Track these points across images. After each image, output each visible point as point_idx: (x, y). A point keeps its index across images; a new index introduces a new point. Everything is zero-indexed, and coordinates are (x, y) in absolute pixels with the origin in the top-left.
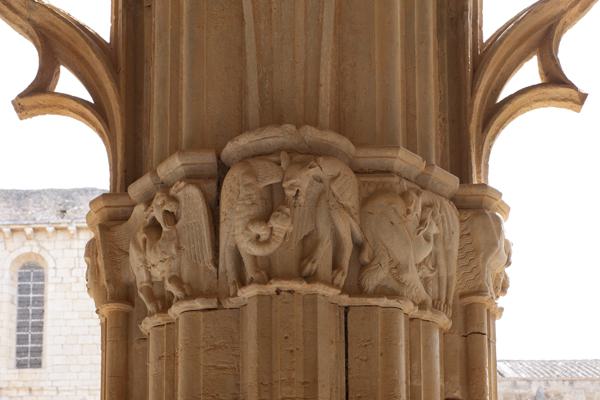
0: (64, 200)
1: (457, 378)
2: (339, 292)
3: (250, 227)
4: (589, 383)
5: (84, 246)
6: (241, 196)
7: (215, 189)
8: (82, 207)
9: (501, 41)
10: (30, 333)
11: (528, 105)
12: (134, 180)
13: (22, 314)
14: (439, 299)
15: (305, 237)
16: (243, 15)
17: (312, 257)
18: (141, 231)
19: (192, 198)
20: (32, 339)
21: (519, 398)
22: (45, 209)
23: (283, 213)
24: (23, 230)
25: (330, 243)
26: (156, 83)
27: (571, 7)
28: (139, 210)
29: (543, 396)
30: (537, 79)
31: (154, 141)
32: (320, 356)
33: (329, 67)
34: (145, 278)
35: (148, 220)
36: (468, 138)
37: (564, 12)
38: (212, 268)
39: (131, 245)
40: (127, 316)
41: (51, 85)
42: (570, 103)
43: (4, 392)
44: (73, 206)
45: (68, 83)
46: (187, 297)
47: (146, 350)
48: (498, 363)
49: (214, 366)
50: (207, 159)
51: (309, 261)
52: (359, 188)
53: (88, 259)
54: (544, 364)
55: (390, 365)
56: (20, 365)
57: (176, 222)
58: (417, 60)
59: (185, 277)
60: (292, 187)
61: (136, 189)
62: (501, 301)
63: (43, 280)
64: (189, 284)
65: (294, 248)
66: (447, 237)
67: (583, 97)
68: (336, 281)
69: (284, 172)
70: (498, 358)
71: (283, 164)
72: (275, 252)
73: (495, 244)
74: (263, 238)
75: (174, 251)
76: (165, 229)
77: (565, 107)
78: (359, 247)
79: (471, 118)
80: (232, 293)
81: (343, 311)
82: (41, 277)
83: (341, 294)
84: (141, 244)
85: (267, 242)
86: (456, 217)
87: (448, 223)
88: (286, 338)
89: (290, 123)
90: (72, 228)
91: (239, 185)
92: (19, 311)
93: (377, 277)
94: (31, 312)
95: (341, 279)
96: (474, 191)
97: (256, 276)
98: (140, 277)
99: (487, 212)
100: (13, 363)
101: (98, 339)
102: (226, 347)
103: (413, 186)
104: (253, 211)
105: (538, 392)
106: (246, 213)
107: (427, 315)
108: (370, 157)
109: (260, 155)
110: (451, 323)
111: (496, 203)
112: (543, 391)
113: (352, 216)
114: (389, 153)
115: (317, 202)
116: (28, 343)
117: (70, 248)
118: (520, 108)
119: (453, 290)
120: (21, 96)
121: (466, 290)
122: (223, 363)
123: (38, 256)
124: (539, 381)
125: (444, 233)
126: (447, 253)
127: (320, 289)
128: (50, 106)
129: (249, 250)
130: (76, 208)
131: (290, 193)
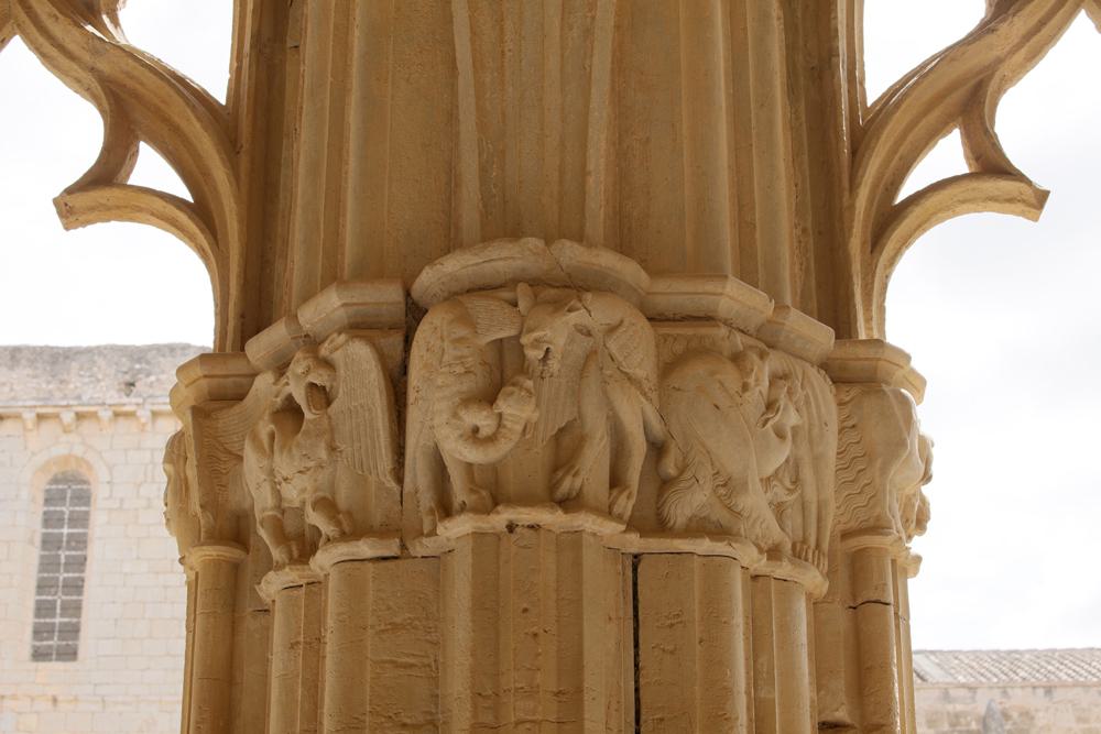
0: (133, 363)
1: (840, 684)
2: (623, 527)
3: (462, 413)
4: (1079, 690)
5: (163, 445)
6: (446, 358)
7: (400, 347)
8: (163, 377)
9: (898, 105)
10: (59, 599)
11: (948, 208)
12: (258, 331)
13: (48, 564)
14: (804, 541)
15: (561, 430)
16: (454, 60)
17: (573, 467)
18: (266, 418)
19: (359, 363)
20: (63, 609)
21: (955, 719)
22: (98, 381)
23: (521, 388)
24: (57, 416)
25: (606, 440)
26: (302, 170)
27: (1013, 52)
28: (263, 382)
29: (998, 716)
30: (962, 167)
31: (296, 263)
32: (587, 644)
33: (603, 145)
34: (270, 502)
35: (279, 400)
36: (847, 260)
37: (1000, 61)
38: (392, 485)
39: (247, 441)
40: (236, 568)
41: (123, 172)
42: (1021, 207)
43: (8, 703)
44: (148, 375)
45: (152, 170)
46: (345, 537)
47: (267, 630)
48: (914, 656)
49: (392, 662)
50: (387, 296)
51: (567, 472)
52: (657, 346)
53: (170, 467)
54: (999, 656)
55: (717, 662)
56: (39, 655)
57: (329, 403)
58: (754, 132)
59: (342, 500)
60: (537, 343)
61: (260, 347)
62: (917, 545)
63: (87, 503)
64: (349, 513)
65: (540, 453)
66: (816, 431)
67: (1042, 197)
68: (617, 510)
69: (523, 318)
70: (914, 647)
71: (522, 305)
72: (505, 457)
73: (901, 444)
74: (485, 432)
75: (323, 454)
76: (308, 415)
77: (1013, 212)
78: (657, 449)
79: (851, 227)
80: (426, 529)
81: (629, 563)
82: (84, 498)
83: (625, 532)
84: (266, 446)
85: (492, 439)
86: (830, 398)
87: (818, 407)
88: (525, 610)
89: (532, 235)
90: (144, 415)
91: (442, 339)
92: (42, 557)
93: (687, 504)
94: (63, 560)
95: (625, 505)
96: (861, 352)
97: (470, 499)
98: (261, 500)
99: (884, 387)
100: (27, 651)
101: (181, 610)
102: (415, 628)
103: (751, 341)
104: (469, 385)
105: (989, 709)
106: (455, 389)
107: (784, 569)
108: (677, 293)
109: (481, 289)
110: (827, 585)
111: (899, 373)
112: (997, 707)
113: (645, 394)
114: (710, 287)
115: (582, 372)
116: (54, 616)
117: (139, 448)
118: (935, 213)
119: (829, 523)
120: (69, 191)
121: (853, 524)
122: (408, 655)
123: (80, 460)
124: (991, 688)
125: (810, 425)
126: (817, 460)
127: (587, 522)
128: (118, 207)
129: (460, 452)
130: (153, 378)
131: (534, 354)
